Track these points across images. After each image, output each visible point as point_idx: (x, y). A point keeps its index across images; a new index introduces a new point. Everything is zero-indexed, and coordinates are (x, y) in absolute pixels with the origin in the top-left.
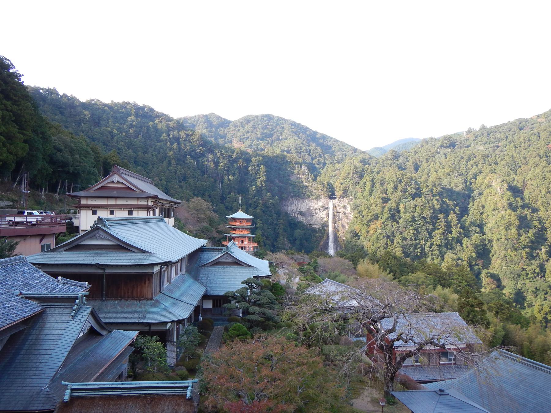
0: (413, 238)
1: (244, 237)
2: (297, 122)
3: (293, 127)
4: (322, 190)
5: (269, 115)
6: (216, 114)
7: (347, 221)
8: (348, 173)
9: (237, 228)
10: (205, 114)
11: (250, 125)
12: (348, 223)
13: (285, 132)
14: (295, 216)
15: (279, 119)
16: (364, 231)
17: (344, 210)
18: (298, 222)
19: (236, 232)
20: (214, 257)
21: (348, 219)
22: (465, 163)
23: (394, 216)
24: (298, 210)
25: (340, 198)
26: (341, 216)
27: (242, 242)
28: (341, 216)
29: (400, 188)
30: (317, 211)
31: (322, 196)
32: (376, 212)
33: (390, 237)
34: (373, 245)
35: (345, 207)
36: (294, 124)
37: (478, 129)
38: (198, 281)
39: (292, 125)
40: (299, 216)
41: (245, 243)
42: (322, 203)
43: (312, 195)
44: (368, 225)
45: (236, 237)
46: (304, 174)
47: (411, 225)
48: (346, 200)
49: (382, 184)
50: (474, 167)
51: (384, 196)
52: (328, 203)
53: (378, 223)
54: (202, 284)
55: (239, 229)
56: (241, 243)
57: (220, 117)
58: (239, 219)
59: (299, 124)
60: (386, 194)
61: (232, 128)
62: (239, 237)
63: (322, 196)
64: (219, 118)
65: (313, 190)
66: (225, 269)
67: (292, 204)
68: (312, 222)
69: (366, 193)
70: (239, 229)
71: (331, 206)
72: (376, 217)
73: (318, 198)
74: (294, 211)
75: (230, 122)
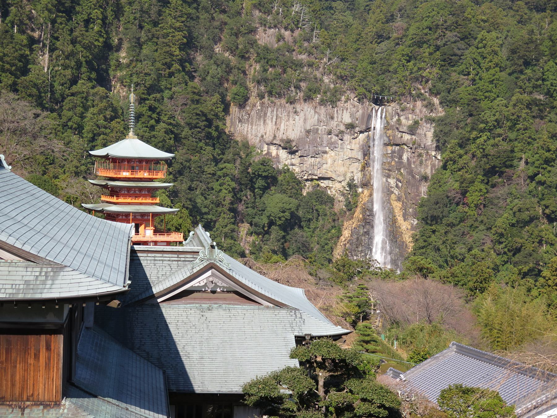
9: (121, 188)
14: (269, 153)
18: (279, 172)
19: (121, 200)
20: (166, 277)
24: (280, 135)
38: (132, 349)
40: (283, 154)
42: (352, 115)
52: (370, 117)
54: (148, 358)
55: (129, 189)
58: (129, 160)
66: (208, 314)
67: (262, 116)
74: (269, 138)
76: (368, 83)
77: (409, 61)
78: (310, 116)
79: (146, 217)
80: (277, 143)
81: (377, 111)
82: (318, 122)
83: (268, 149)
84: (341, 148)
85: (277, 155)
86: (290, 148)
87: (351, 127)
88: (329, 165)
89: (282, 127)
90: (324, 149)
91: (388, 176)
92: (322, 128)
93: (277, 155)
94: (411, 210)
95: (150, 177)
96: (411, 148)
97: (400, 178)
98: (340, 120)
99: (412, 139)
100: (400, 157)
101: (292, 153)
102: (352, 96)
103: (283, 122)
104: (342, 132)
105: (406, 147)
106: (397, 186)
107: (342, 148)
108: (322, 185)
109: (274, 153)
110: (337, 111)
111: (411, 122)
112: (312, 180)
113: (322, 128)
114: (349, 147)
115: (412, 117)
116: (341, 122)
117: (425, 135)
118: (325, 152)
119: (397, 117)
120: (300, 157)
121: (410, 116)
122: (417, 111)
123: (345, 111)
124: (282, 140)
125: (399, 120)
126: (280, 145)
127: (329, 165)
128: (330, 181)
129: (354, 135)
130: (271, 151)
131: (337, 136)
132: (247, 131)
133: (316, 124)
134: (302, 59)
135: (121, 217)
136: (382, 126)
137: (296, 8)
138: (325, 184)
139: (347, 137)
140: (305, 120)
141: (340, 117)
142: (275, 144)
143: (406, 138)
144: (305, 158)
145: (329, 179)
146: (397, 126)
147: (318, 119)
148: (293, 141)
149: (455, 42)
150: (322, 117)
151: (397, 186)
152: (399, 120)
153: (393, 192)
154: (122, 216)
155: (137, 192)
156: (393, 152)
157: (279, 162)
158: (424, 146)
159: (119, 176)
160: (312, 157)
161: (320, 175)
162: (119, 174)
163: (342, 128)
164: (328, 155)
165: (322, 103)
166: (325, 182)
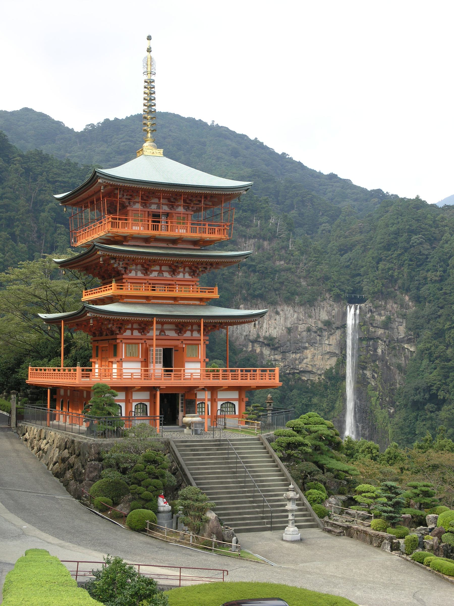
1: (182, 325)
9: (131, 260)
14: (253, 351)
27: (168, 359)
40: (266, 351)
41: (193, 371)
42: (329, 313)
45: (122, 322)
56: (157, 368)
59: (243, 137)
62: (143, 324)
68: (302, 367)
71: (350, 321)
76: (341, 284)
77: (378, 263)
78: (289, 315)
79: (188, 334)
80: (261, 340)
81: (350, 308)
82: (297, 321)
83: (253, 346)
84: (320, 344)
86: (273, 345)
87: (328, 324)
88: (308, 360)
89: (265, 326)
90: (303, 345)
91: (364, 368)
92: (301, 327)
93: (262, 352)
94: (387, 399)
95: (197, 235)
96: (385, 342)
97: (376, 369)
98: (317, 318)
99: (385, 333)
100: (375, 350)
101: (275, 349)
102: (327, 295)
103: (265, 321)
104: (321, 329)
105: (380, 341)
106: (373, 377)
107: (321, 344)
108: (304, 378)
109: (258, 350)
110: (315, 309)
111: (383, 318)
112: (294, 373)
113: (301, 327)
114: (327, 342)
115: (385, 313)
116: (319, 320)
117: (397, 329)
118: (306, 348)
119: (370, 314)
120: (282, 352)
121: (383, 312)
122: (389, 306)
123: (322, 310)
124: (265, 338)
125: (372, 316)
126: (263, 343)
127: (308, 360)
128: (311, 375)
129: (331, 331)
130: (255, 348)
131: (315, 332)
132: (233, 331)
133: (296, 322)
134: (281, 265)
136: (357, 322)
137: (272, 221)
138: (306, 377)
139: (325, 334)
140: (286, 319)
141: (317, 315)
142: (259, 341)
143: (380, 333)
144: (287, 354)
145: (310, 372)
146: (371, 322)
147: (297, 318)
148: (275, 338)
149: (421, 243)
150: (301, 316)
151: (373, 377)
152: (372, 316)
153: (369, 383)
154: (132, 329)
155: (166, 275)
156: (368, 346)
157: (263, 358)
158: (397, 338)
160: (293, 353)
161: (302, 369)
162: (124, 226)
163: (320, 325)
164: (308, 351)
165: (301, 304)
166: (306, 375)
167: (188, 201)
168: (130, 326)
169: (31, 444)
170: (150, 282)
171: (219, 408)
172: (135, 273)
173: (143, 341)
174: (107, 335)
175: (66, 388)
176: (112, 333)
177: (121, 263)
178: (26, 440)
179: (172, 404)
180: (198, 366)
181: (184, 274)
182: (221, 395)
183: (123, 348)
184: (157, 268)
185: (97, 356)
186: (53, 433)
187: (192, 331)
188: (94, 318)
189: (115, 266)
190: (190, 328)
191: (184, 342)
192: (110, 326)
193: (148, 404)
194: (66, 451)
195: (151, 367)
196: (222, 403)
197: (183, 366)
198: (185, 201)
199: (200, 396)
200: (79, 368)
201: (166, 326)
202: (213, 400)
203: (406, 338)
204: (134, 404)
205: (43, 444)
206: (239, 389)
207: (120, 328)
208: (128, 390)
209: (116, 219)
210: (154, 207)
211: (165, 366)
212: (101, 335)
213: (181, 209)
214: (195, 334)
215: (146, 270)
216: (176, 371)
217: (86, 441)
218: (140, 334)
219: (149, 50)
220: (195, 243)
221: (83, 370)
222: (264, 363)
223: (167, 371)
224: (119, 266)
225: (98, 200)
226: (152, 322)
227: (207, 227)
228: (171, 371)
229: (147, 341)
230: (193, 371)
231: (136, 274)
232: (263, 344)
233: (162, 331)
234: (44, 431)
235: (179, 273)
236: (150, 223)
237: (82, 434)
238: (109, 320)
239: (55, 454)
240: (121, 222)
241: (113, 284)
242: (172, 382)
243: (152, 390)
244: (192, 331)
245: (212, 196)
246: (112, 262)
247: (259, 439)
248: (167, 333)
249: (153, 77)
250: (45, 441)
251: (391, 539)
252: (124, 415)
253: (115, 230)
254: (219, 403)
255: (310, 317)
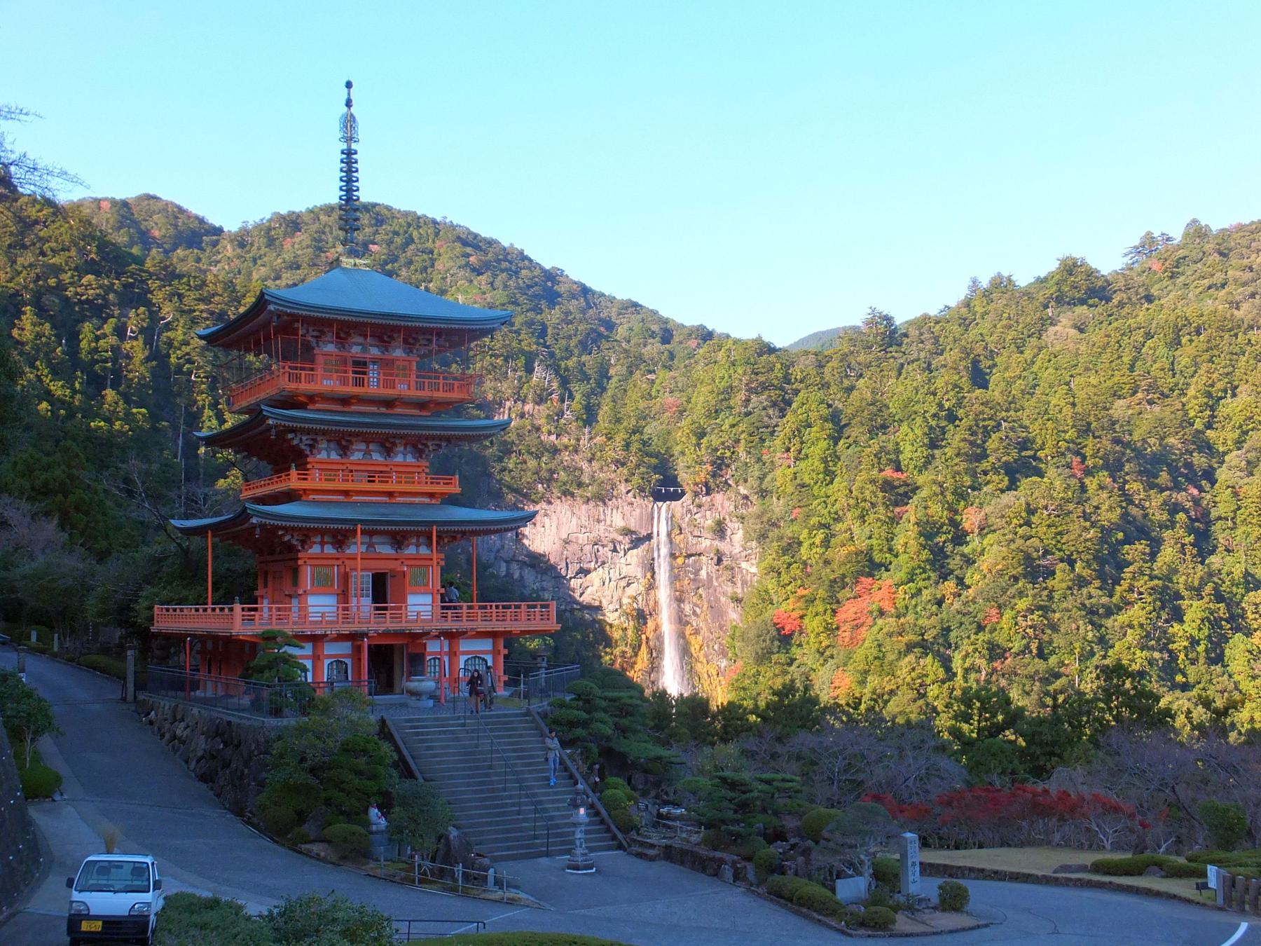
0: (1034, 647)
2: (485, 231)
3: (469, 250)
4: (620, 463)
5: (375, 205)
6: (165, 196)
7: (729, 589)
8: (729, 391)
9: (316, 434)
10: (120, 195)
11: (301, 237)
12: (738, 600)
13: (439, 265)
14: (509, 574)
15: (416, 221)
16: (813, 624)
17: (716, 543)
19: (315, 480)
21: (732, 580)
22: (1162, 351)
23: (942, 551)
25: (696, 494)
26: (707, 568)
27: (381, 589)
28: (707, 568)
29: (956, 438)
30: (605, 552)
31: (623, 488)
32: (861, 544)
33: (937, 646)
34: (863, 683)
35: (720, 530)
36: (470, 241)
37: (1177, 234)
39: (465, 243)
41: (420, 607)
43: (580, 485)
44: (834, 602)
46: (540, 400)
47: (1021, 594)
48: (723, 503)
49: (880, 427)
50: (1204, 367)
51: (889, 473)
53: (885, 589)
56: (364, 604)
57: (181, 210)
59: (491, 243)
60: (898, 469)
61: (229, 250)
62: (340, 536)
63: (623, 488)
64: (176, 213)
65: (585, 465)
69: (810, 469)
70: (343, 442)
72: (871, 566)
73: (603, 497)
75: (218, 231)
79: (411, 551)
81: (659, 509)
83: (508, 568)
85: (521, 577)
88: (594, 588)
93: (521, 577)
94: (716, 647)
95: (426, 394)
100: (697, 573)
109: (516, 575)
135: (316, 549)
149: (764, 409)
150: (584, 521)
151: (694, 613)
154: (322, 544)
155: (377, 457)
157: (525, 587)
159: (305, 387)
162: (311, 379)
167: (411, 340)
168: (318, 539)
169: (159, 729)
170: (351, 467)
171: (462, 666)
172: (325, 454)
173: (339, 562)
174: (281, 553)
175: (215, 638)
176: (291, 548)
177: (304, 438)
178: (151, 723)
179: (388, 660)
180: (428, 599)
181: (405, 455)
182: (465, 646)
183: (307, 574)
184: (363, 446)
185: (266, 587)
186: (195, 711)
187: (418, 546)
188: (262, 526)
189: (295, 442)
190: (414, 541)
191: (406, 562)
192: (286, 538)
193: (348, 661)
194: (218, 739)
195: (353, 602)
196: (466, 657)
197: (404, 601)
198: (406, 342)
199: (433, 647)
200: (238, 607)
201: (375, 539)
202: (453, 654)
203: (744, 554)
204: (327, 662)
205: (180, 730)
206: (493, 635)
207: (303, 542)
208: (316, 639)
209: (296, 368)
210: (356, 350)
211: (375, 600)
212: (272, 553)
213: (398, 353)
214: (424, 550)
215: (344, 450)
216: (393, 608)
217: (248, 723)
218: (334, 551)
219: (349, 103)
220: (422, 405)
221: (243, 609)
222: (527, 592)
223: (377, 609)
224: (302, 442)
225: (267, 338)
226: (355, 531)
227: (441, 381)
228: (386, 609)
229: (346, 562)
230: (420, 607)
231: (329, 455)
232: (523, 564)
233: (371, 545)
234: (181, 707)
235: (396, 455)
236: (351, 375)
237: (243, 710)
238: (285, 528)
239: (201, 744)
240: (303, 373)
241: (293, 472)
242: (389, 624)
243: (353, 637)
244: (418, 546)
245: (449, 333)
246: (290, 436)
247: (528, 713)
248: (379, 549)
249: (354, 146)
250: (182, 725)
251: (734, 863)
252: (310, 680)
253: (293, 386)
254: (462, 659)
255: (599, 521)
